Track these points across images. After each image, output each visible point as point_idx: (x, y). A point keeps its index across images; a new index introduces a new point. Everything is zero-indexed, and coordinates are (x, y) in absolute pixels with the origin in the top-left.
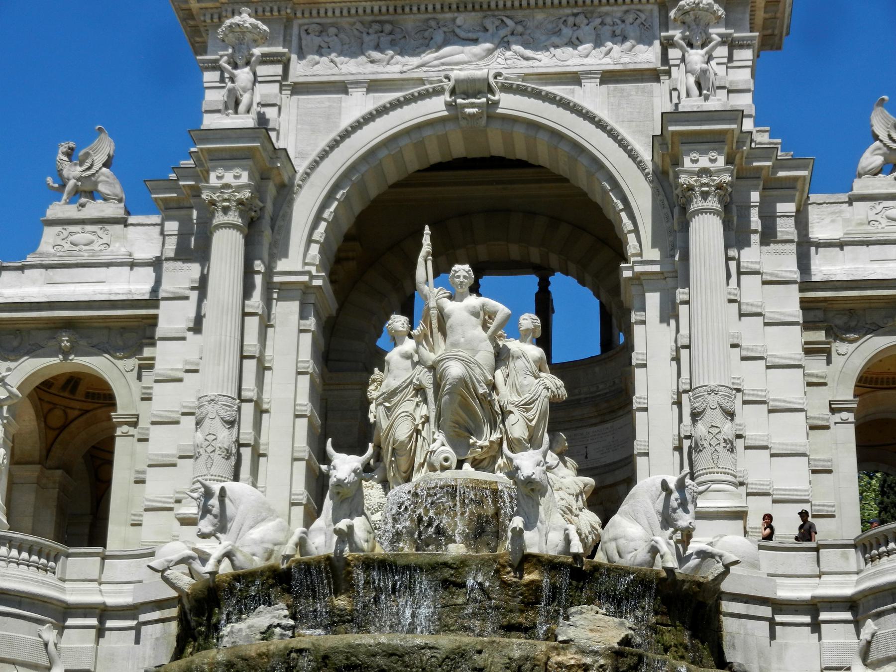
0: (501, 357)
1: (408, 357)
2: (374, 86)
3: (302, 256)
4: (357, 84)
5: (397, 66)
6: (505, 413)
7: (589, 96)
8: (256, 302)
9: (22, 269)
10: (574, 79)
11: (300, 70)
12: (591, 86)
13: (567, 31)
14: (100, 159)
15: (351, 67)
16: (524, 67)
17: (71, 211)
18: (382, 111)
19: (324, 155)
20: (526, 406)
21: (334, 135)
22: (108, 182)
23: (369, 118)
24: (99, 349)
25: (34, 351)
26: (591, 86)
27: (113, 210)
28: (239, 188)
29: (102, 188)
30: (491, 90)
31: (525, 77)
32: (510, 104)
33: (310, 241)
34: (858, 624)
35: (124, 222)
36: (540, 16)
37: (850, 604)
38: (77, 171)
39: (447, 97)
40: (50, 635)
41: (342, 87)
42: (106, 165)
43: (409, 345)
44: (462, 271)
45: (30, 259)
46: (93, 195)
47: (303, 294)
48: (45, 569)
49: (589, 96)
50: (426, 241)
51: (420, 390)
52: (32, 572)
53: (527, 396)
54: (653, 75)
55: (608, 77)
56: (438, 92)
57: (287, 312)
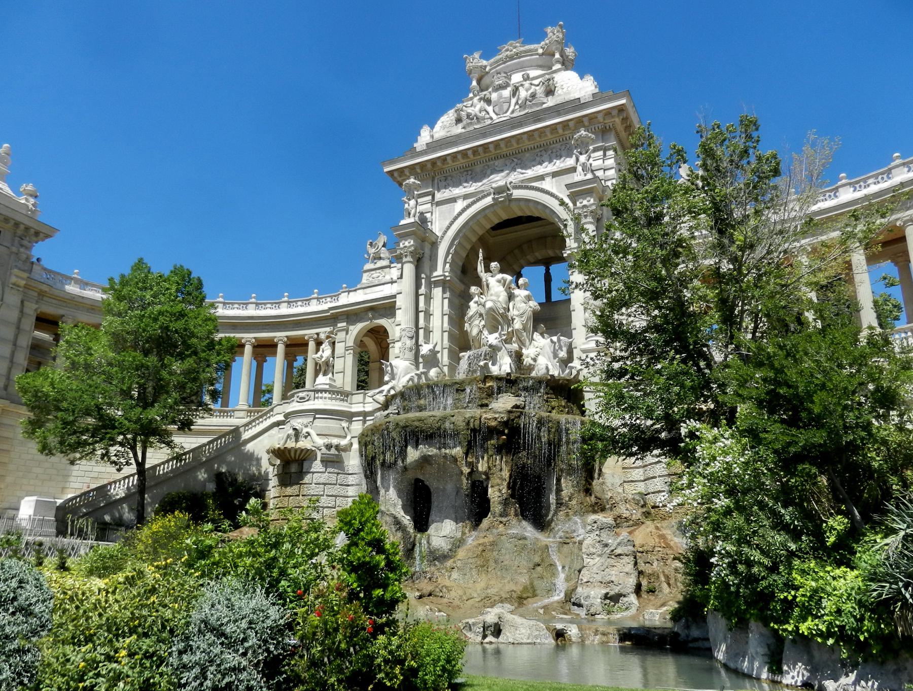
0: (511, 297)
1: (476, 302)
2: (465, 197)
3: (442, 270)
4: (459, 197)
5: (472, 187)
6: (513, 320)
8: (422, 290)
9: (355, 290)
10: (541, 178)
11: (439, 196)
13: (538, 159)
14: (381, 244)
16: (521, 177)
17: (372, 266)
18: (469, 206)
19: (448, 228)
20: (521, 315)
21: (451, 219)
22: (384, 253)
23: (464, 210)
24: (383, 316)
25: (360, 321)
26: (548, 179)
28: (410, 247)
29: (382, 255)
30: (509, 190)
31: (522, 181)
32: (517, 193)
33: (445, 263)
35: (389, 267)
36: (527, 155)
39: (492, 196)
40: (345, 424)
41: (453, 200)
42: (384, 246)
44: (494, 265)
45: (359, 286)
46: (380, 258)
47: (444, 284)
48: (343, 400)
49: (547, 184)
50: (481, 255)
51: (481, 315)
52: (338, 403)
53: (521, 311)
55: (555, 175)
56: (489, 195)
57: (437, 292)
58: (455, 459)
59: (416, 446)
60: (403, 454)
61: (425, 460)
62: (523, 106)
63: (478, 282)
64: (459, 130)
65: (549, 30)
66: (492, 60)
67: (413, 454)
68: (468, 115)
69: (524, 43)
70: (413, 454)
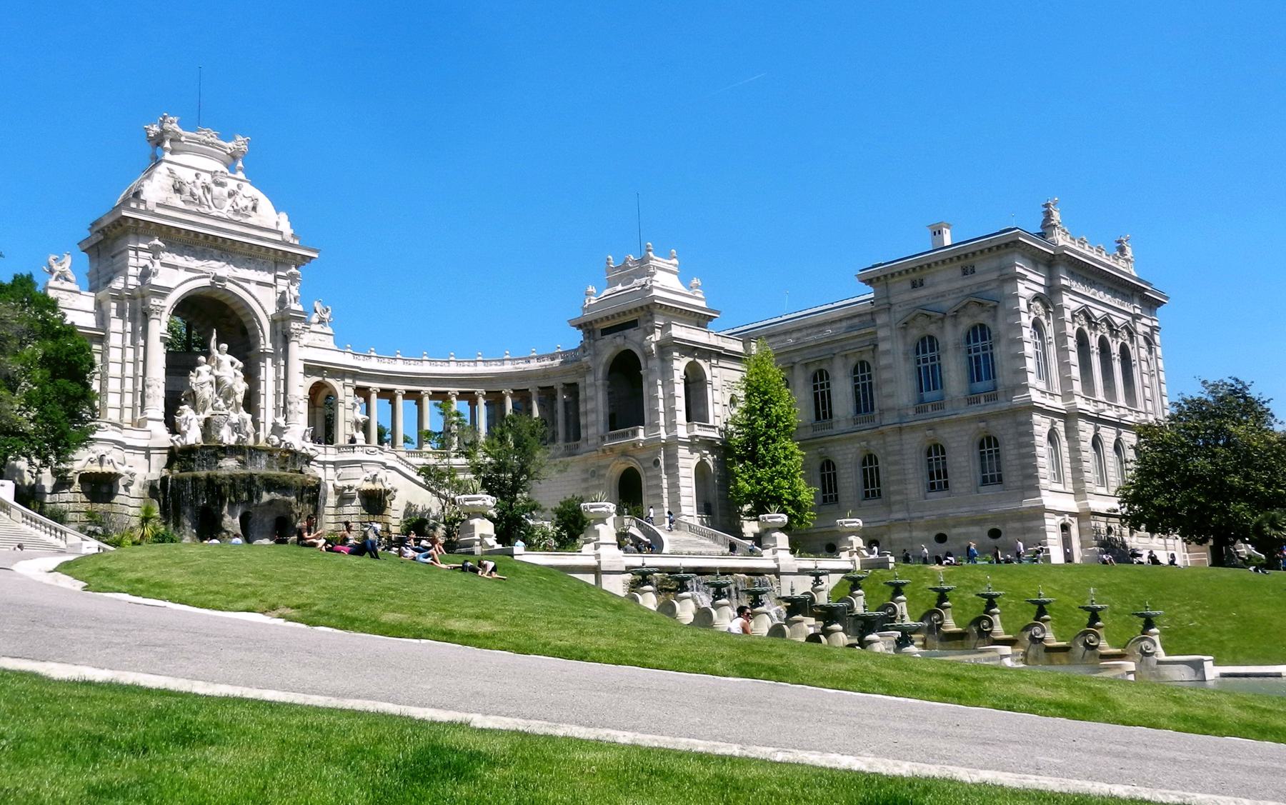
2: (187, 269)
5: (194, 263)
7: (252, 288)
10: (248, 281)
12: (253, 285)
15: (179, 260)
16: (235, 274)
17: (57, 284)
27: (76, 288)
32: (230, 286)
34: (335, 469)
37: (333, 463)
38: (60, 268)
41: (176, 267)
43: (208, 367)
44: (225, 346)
49: (252, 288)
54: (270, 285)
55: (259, 283)
58: (290, 503)
59: (269, 491)
60: (259, 497)
61: (271, 502)
62: (236, 212)
63: (208, 354)
64: (176, 201)
65: (239, 138)
66: (189, 134)
67: (266, 497)
68: (192, 195)
69: (220, 137)
70: (266, 497)
